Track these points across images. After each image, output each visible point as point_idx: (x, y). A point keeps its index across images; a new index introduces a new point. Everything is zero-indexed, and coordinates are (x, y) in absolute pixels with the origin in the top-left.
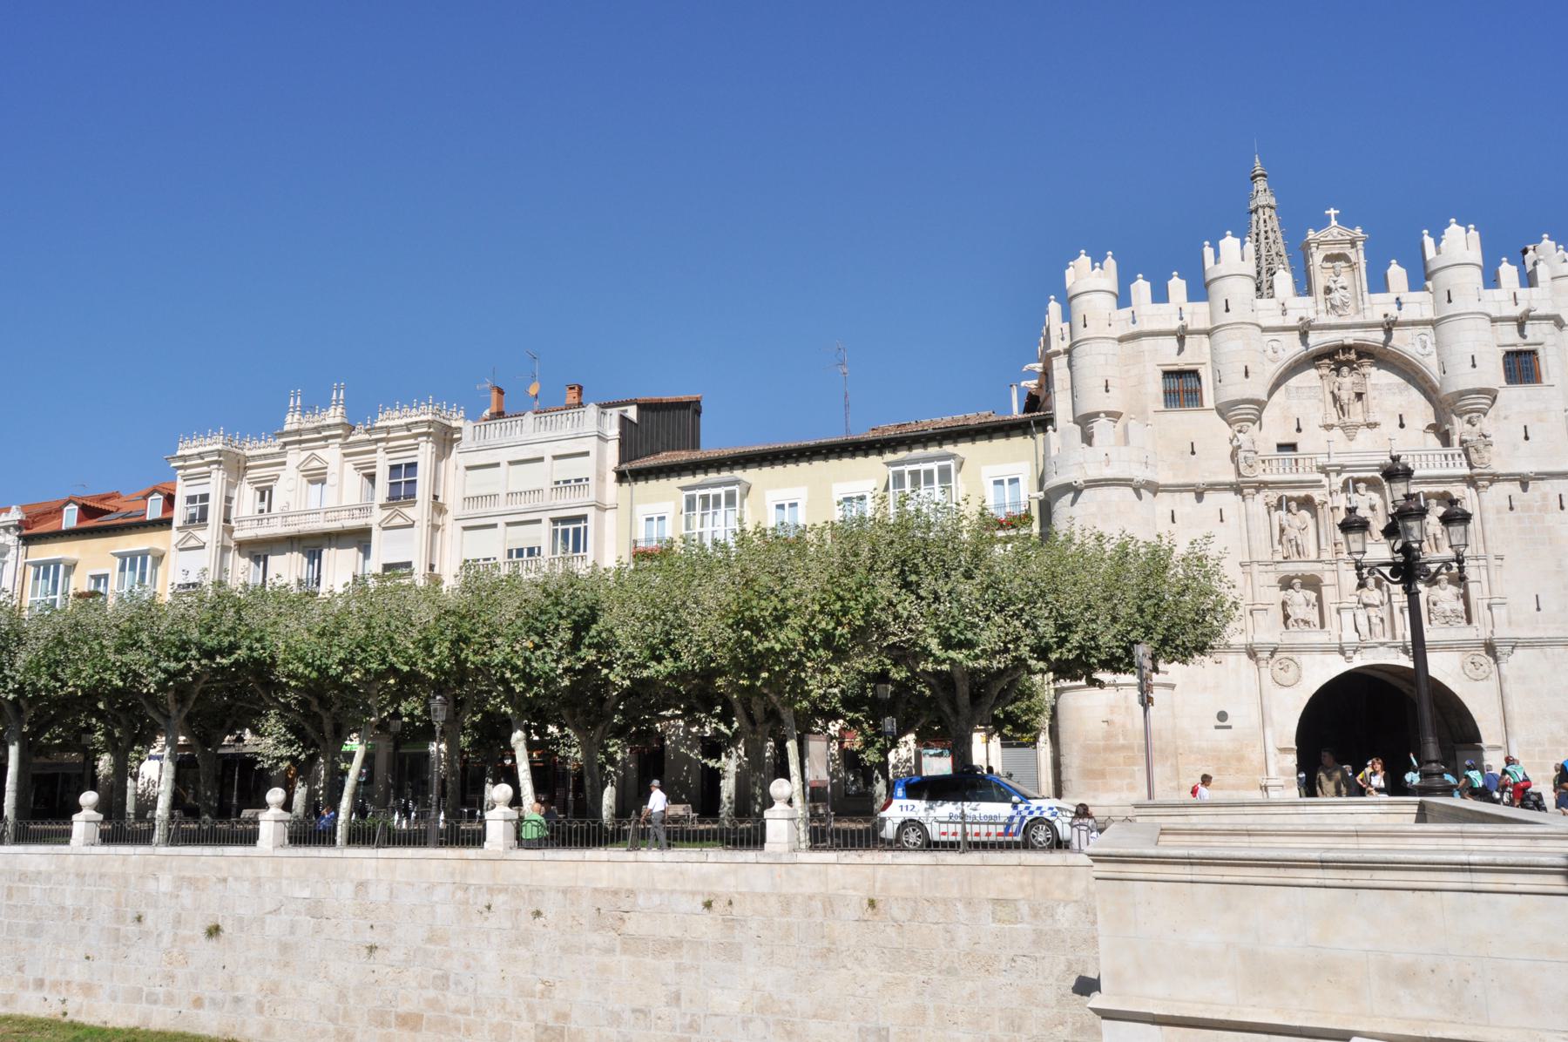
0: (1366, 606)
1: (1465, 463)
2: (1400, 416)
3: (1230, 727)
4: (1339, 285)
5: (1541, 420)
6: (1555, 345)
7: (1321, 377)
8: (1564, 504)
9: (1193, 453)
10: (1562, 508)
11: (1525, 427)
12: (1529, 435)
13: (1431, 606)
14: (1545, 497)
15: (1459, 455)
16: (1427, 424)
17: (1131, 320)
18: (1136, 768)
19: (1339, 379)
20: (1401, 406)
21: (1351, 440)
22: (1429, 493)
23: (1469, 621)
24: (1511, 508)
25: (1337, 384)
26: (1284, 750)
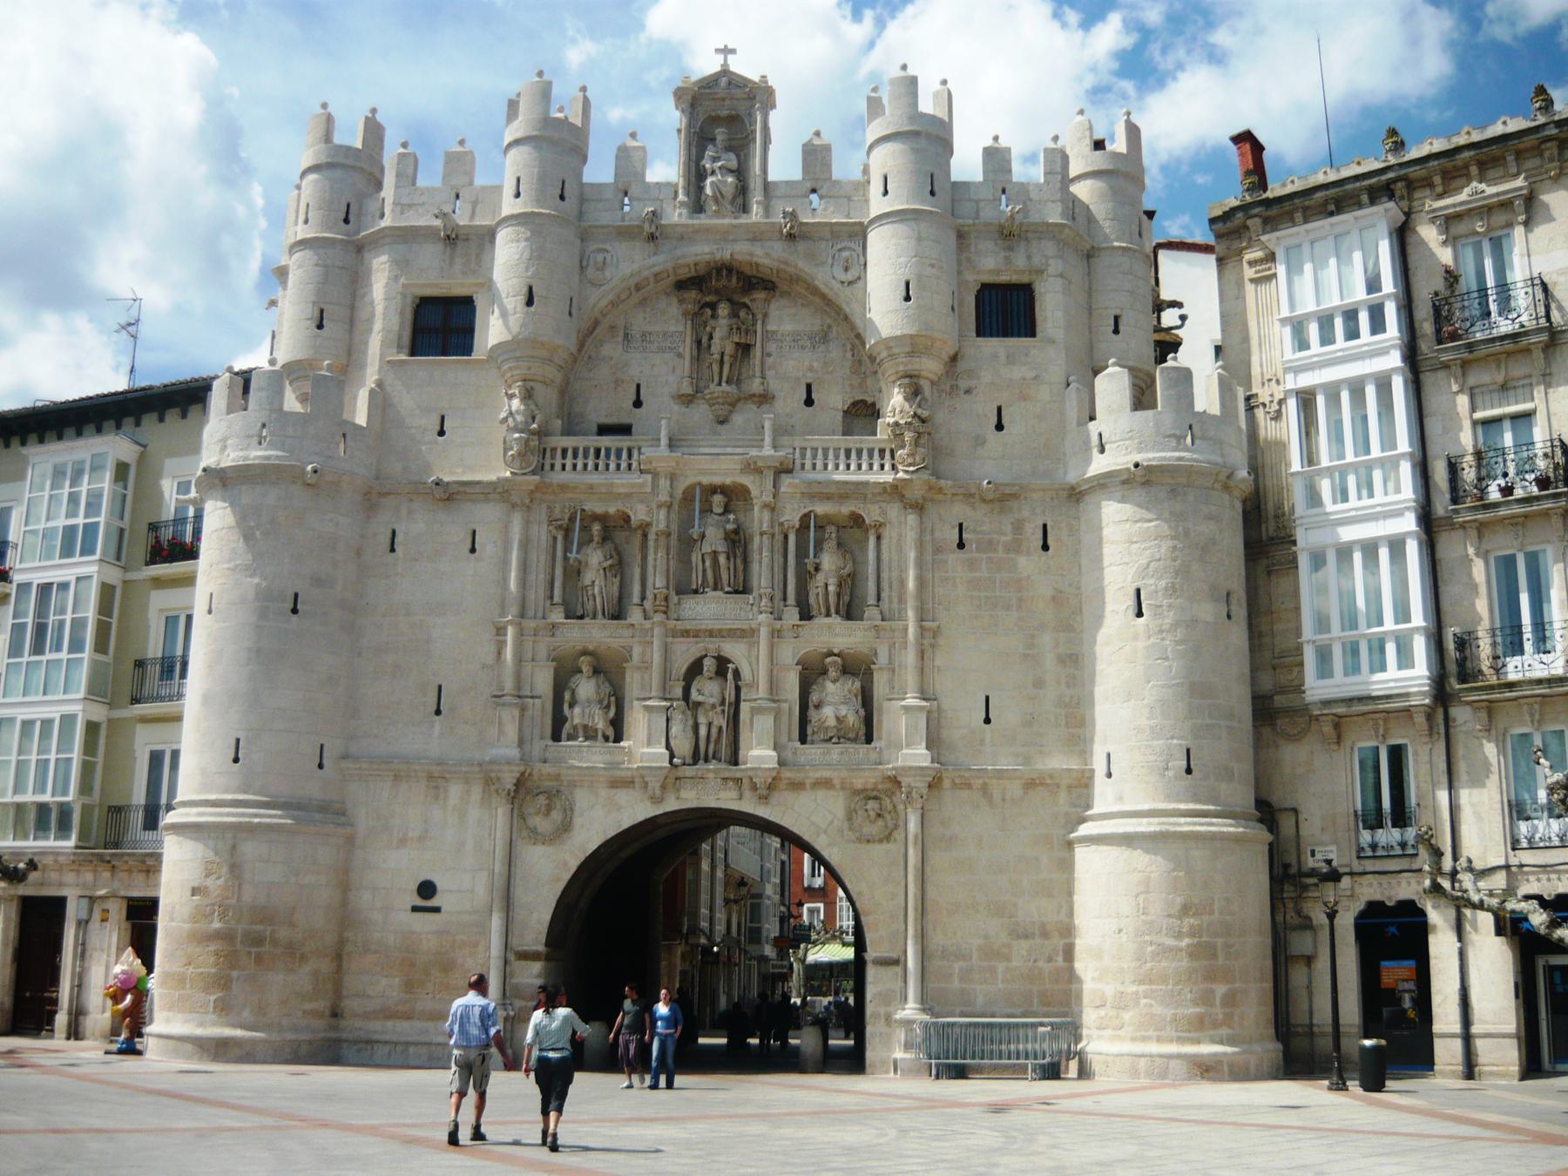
0: (698, 704)
1: (887, 467)
2: (809, 387)
3: (437, 910)
4: (719, 164)
5: (1024, 398)
6: (1061, 275)
7: (685, 314)
8: (1050, 541)
9: (441, 433)
10: (1045, 547)
11: (999, 409)
12: (1005, 421)
13: (812, 713)
14: (1018, 527)
15: (882, 452)
16: (852, 400)
17: (378, 214)
18: (235, 974)
19: (712, 322)
20: (811, 369)
21: (721, 422)
22: (826, 516)
23: (869, 739)
24: (961, 545)
25: (708, 329)
26: (524, 956)
